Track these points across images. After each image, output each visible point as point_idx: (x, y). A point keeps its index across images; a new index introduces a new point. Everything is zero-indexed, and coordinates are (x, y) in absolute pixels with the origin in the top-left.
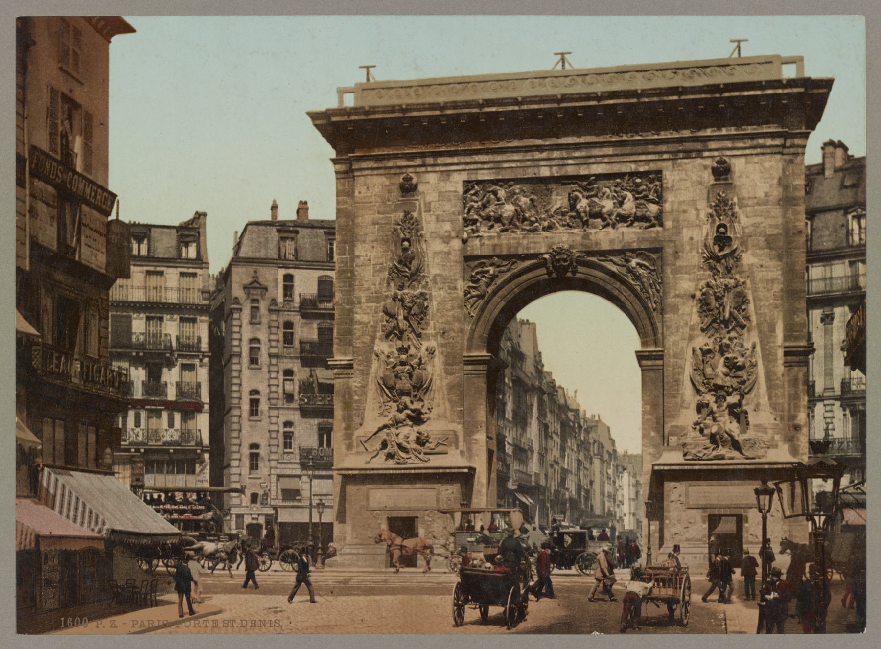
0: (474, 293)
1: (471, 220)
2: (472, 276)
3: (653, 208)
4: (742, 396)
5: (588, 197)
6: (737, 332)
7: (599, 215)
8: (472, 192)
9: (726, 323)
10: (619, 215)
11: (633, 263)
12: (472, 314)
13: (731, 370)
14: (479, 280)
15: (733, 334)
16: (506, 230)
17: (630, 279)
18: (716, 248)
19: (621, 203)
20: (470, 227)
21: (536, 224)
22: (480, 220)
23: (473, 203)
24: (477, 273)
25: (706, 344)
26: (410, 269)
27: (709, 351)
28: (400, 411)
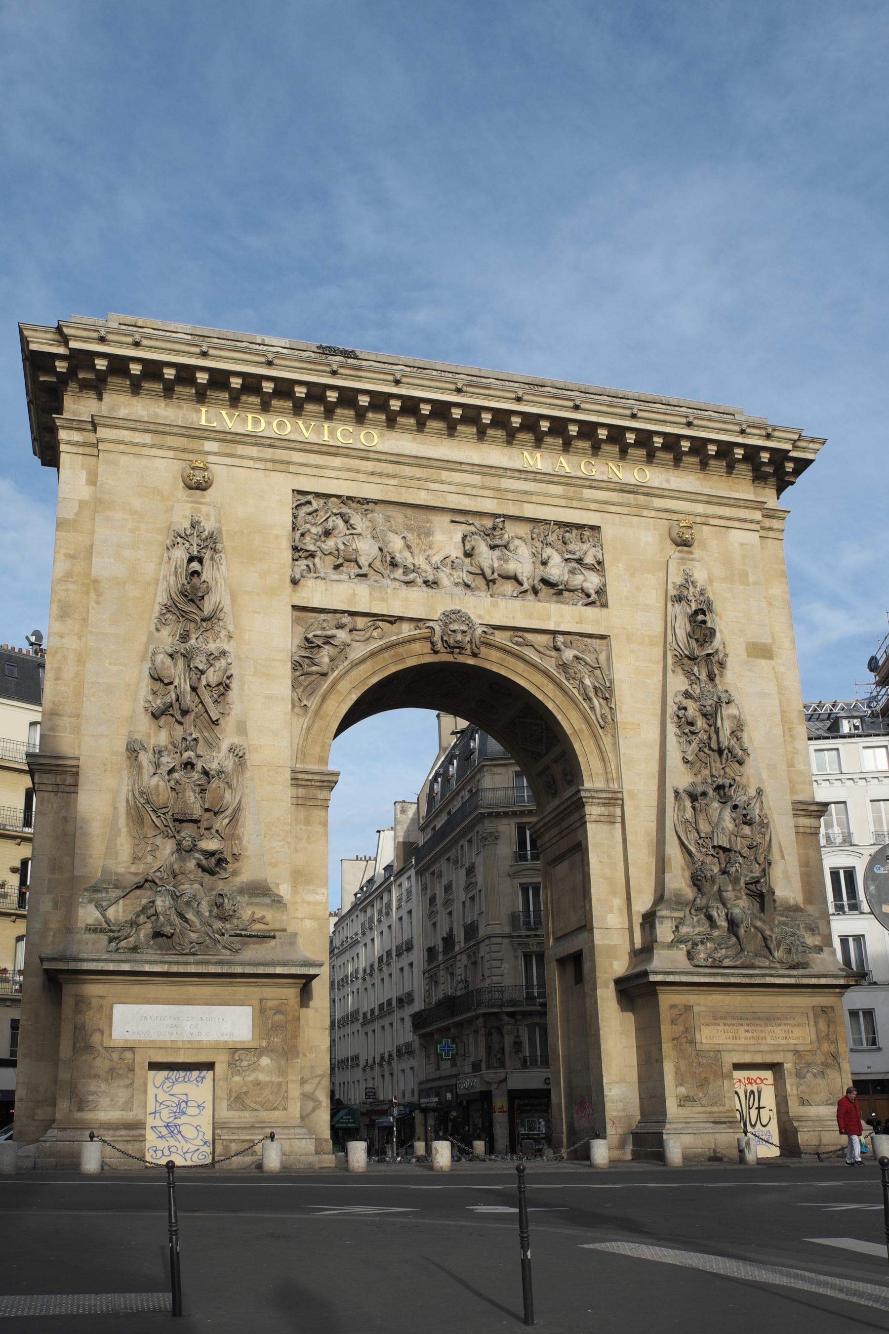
1: (307, 551)
2: (307, 639)
5: (493, 547)
14: (319, 647)
19: (544, 563)
20: (305, 562)
21: (415, 574)
22: (319, 553)
23: (308, 526)
25: (693, 784)
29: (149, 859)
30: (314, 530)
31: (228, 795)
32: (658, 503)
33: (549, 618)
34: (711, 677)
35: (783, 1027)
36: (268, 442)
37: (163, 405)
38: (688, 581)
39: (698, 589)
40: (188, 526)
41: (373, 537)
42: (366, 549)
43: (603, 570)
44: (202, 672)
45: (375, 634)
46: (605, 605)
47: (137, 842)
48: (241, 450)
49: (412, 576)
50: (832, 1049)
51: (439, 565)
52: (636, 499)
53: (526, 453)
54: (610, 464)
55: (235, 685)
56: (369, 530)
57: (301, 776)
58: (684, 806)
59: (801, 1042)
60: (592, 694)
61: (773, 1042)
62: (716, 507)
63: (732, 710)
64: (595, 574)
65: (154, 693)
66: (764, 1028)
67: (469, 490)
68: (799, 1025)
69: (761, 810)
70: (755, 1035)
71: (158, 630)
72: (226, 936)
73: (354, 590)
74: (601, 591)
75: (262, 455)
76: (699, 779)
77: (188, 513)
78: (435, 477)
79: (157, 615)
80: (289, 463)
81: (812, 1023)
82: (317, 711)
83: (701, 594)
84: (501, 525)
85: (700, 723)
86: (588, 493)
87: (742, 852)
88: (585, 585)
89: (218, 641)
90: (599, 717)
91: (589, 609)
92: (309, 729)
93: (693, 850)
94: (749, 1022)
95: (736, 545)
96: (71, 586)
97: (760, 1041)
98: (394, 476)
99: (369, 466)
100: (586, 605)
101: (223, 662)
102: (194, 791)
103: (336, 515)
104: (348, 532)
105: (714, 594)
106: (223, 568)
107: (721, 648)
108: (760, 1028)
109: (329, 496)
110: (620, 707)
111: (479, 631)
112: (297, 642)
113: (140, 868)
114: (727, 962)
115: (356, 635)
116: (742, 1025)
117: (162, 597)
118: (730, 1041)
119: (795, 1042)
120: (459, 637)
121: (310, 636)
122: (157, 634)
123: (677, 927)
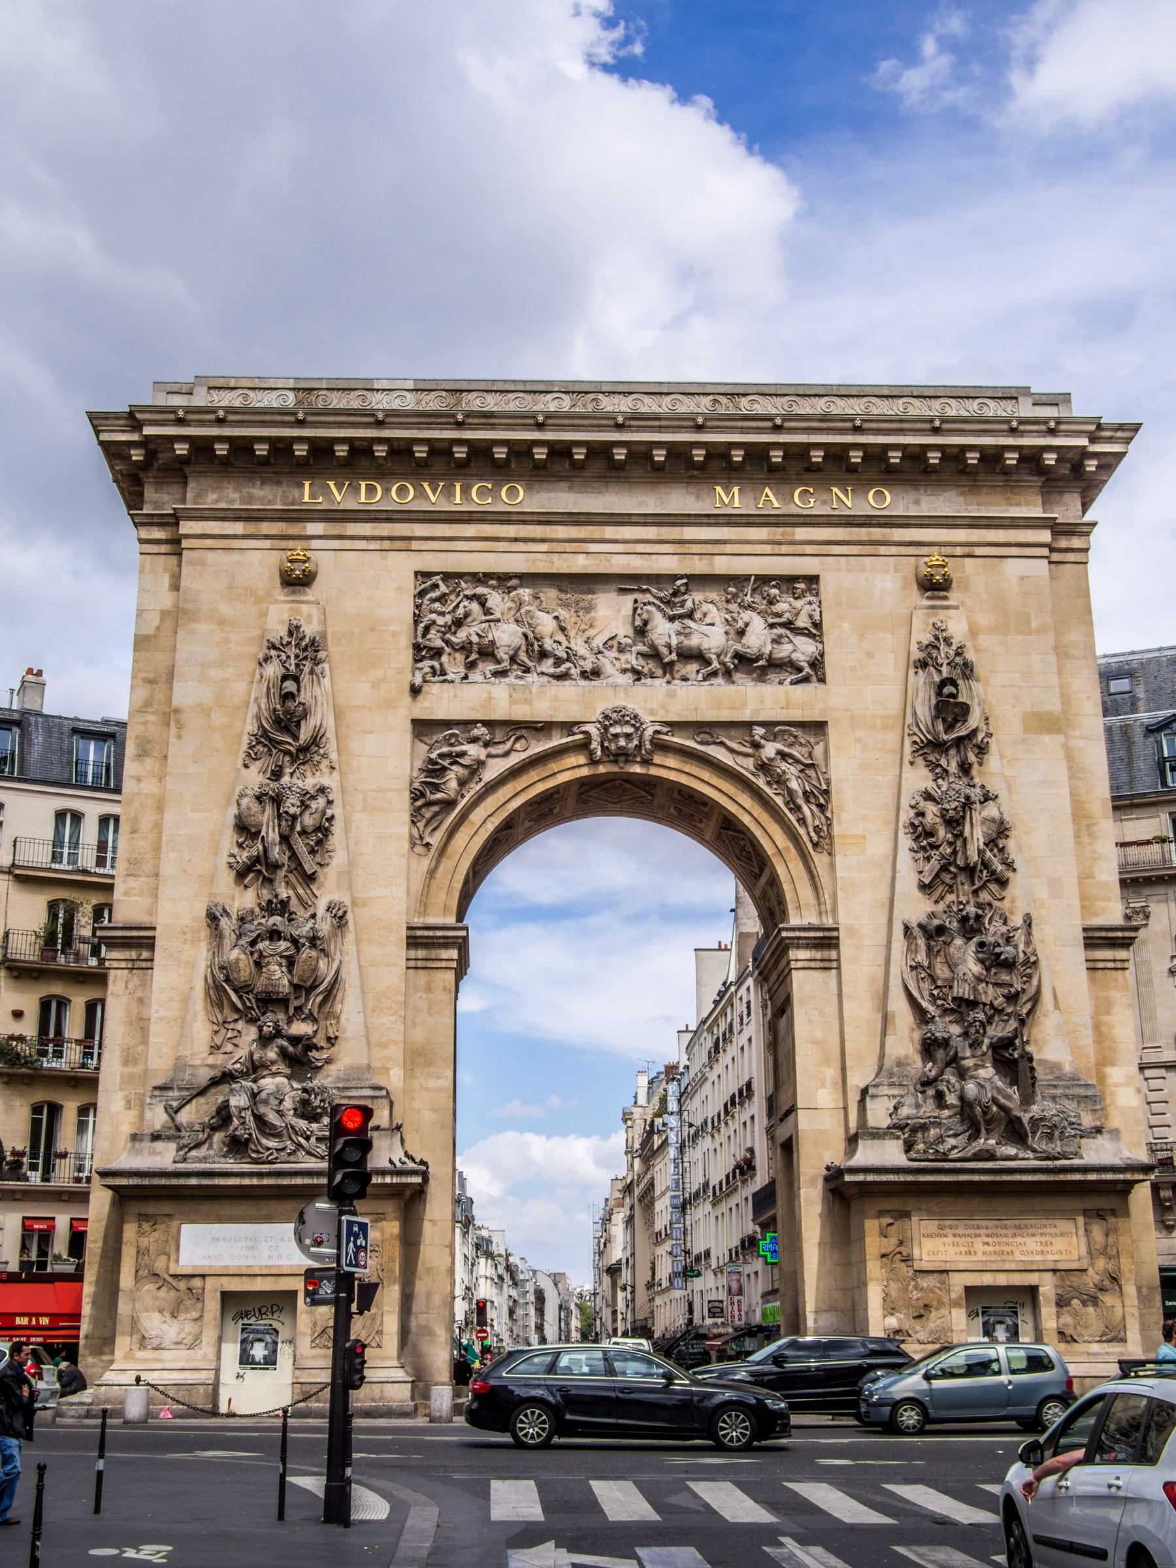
0: (433, 797)
1: (430, 649)
2: (432, 762)
3: (803, 649)
4: (1022, 1022)
5: (672, 619)
6: (992, 894)
7: (698, 656)
8: (433, 595)
9: (970, 871)
10: (737, 656)
11: (770, 750)
12: (427, 839)
13: (988, 969)
14: (444, 769)
15: (984, 896)
16: (503, 673)
17: (761, 782)
18: (940, 727)
19: (741, 633)
21: (568, 665)
23: (433, 616)
24: (441, 756)
25: (932, 915)
26: (296, 738)
27: (941, 930)
28: (264, 1040)
29: (229, 1047)
30: (441, 621)
31: (322, 964)
32: (898, 534)
33: (744, 705)
34: (965, 769)
35: (1038, 1238)
36: (384, 516)
37: (259, 483)
38: (940, 638)
39: (954, 647)
40: (283, 632)
41: (517, 621)
42: (507, 636)
43: (821, 635)
44: (294, 817)
45: (518, 746)
46: (822, 680)
47: (216, 1028)
48: (352, 529)
49: (563, 668)
50: (1110, 1266)
51: (601, 649)
52: (869, 534)
53: (719, 489)
54: (835, 489)
55: (337, 828)
56: (512, 612)
57: (419, 933)
58: (916, 945)
59: (1064, 1257)
60: (800, 801)
61: (1023, 1258)
62: (984, 532)
63: (991, 810)
64: (811, 641)
65: (240, 845)
66: (1011, 1240)
67: (641, 548)
68: (1062, 1235)
69: (1028, 943)
70: (997, 1248)
71: (246, 766)
72: (313, 1140)
73: (490, 693)
74: (817, 664)
75: (377, 533)
76: (941, 906)
77: (286, 617)
78: (596, 536)
79: (245, 747)
80: (410, 538)
81: (1081, 1232)
82: (442, 851)
83: (957, 654)
84: (683, 589)
85: (942, 833)
86: (802, 533)
87: (996, 1003)
88: (794, 656)
89: (318, 774)
90: (811, 830)
91: (799, 687)
92: (432, 873)
93: (924, 1004)
94: (989, 1232)
95: (1014, 580)
96: (151, 718)
97: (1004, 1257)
98: (543, 540)
99: (511, 531)
100: (796, 683)
101: (321, 801)
102: (280, 965)
103: (466, 597)
104: (484, 618)
105: (977, 650)
106: (326, 681)
107: (983, 727)
108: (1005, 1240)
109: (460, 575)
110: (839, 817)
111: (649, 732)
112: (419, 764)
113: (218, 1059)
114: (954, 1154)
115: (493, 750)
116: (979, 1236)
117: (251, 727)
118: (962, 1258)
119: (1056, 1257)
120: (622, 742)
121: (434, 756)
122: (244, 771)
123: (896, 1108)
